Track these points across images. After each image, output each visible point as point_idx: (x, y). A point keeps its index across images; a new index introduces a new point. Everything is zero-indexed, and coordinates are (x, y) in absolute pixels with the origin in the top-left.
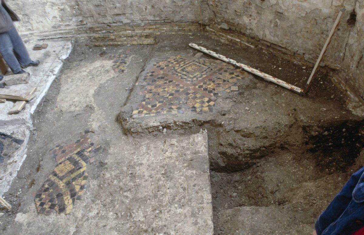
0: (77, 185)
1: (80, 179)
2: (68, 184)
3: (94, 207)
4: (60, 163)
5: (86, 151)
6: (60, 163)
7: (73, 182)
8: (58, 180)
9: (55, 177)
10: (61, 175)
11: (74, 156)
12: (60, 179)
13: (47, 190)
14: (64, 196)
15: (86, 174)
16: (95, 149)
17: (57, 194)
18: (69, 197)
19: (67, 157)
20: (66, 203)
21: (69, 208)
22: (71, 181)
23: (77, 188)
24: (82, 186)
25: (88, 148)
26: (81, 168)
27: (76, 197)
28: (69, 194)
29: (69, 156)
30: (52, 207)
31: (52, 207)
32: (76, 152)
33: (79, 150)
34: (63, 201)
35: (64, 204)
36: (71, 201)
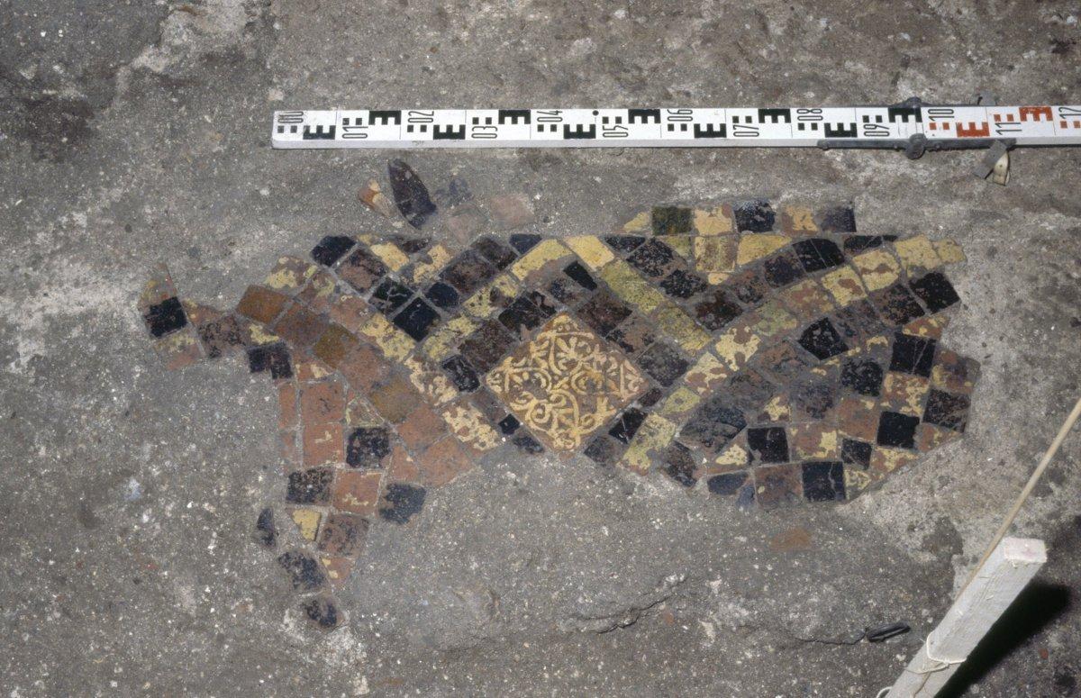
0: (731, 256)
1: (681, 251)
2: (720, 311)
3: (868, 173)
4: (509, 425)
5: (407, 271)
6: (509, 425)
7: (705, 286)
8: (682, 393)
9: (655, 419)
10: (631, 382)
11: (438, 345)
12: (668, 383)
13: (770, 443)
14: (827, 309)
15: (640, 224)
16: (405, 209)
17: (812, 358)
18: (832, 278)
19: (450, 394)
20: (877, 282)
21: (917, 253)
22: (698, 298)
23: (754, 248)
24: (741, 228)
25: (377, 268)
26: (577, 271)
27: (838, 238)
28: (811, 283)
29: (441, 380)
30: (916, 357)
31: (916, 357)
32: (399, 346)
33: (378, 329)
34: (866, 310)
35: (897, 288)
36: (871, 258)
